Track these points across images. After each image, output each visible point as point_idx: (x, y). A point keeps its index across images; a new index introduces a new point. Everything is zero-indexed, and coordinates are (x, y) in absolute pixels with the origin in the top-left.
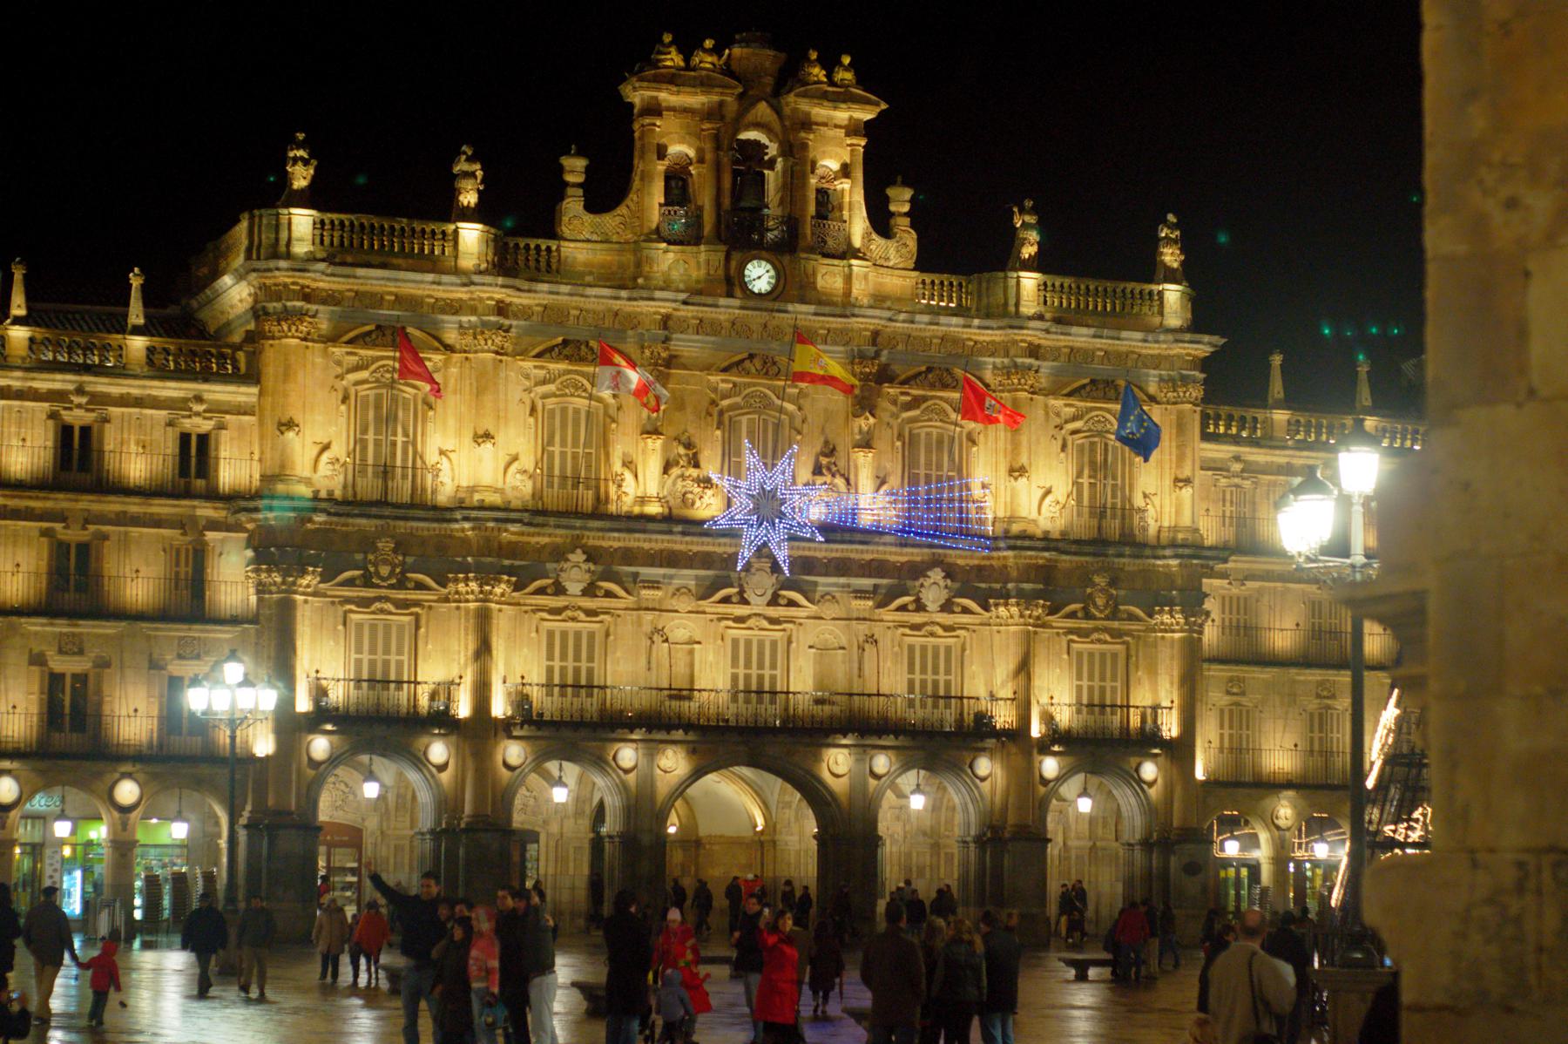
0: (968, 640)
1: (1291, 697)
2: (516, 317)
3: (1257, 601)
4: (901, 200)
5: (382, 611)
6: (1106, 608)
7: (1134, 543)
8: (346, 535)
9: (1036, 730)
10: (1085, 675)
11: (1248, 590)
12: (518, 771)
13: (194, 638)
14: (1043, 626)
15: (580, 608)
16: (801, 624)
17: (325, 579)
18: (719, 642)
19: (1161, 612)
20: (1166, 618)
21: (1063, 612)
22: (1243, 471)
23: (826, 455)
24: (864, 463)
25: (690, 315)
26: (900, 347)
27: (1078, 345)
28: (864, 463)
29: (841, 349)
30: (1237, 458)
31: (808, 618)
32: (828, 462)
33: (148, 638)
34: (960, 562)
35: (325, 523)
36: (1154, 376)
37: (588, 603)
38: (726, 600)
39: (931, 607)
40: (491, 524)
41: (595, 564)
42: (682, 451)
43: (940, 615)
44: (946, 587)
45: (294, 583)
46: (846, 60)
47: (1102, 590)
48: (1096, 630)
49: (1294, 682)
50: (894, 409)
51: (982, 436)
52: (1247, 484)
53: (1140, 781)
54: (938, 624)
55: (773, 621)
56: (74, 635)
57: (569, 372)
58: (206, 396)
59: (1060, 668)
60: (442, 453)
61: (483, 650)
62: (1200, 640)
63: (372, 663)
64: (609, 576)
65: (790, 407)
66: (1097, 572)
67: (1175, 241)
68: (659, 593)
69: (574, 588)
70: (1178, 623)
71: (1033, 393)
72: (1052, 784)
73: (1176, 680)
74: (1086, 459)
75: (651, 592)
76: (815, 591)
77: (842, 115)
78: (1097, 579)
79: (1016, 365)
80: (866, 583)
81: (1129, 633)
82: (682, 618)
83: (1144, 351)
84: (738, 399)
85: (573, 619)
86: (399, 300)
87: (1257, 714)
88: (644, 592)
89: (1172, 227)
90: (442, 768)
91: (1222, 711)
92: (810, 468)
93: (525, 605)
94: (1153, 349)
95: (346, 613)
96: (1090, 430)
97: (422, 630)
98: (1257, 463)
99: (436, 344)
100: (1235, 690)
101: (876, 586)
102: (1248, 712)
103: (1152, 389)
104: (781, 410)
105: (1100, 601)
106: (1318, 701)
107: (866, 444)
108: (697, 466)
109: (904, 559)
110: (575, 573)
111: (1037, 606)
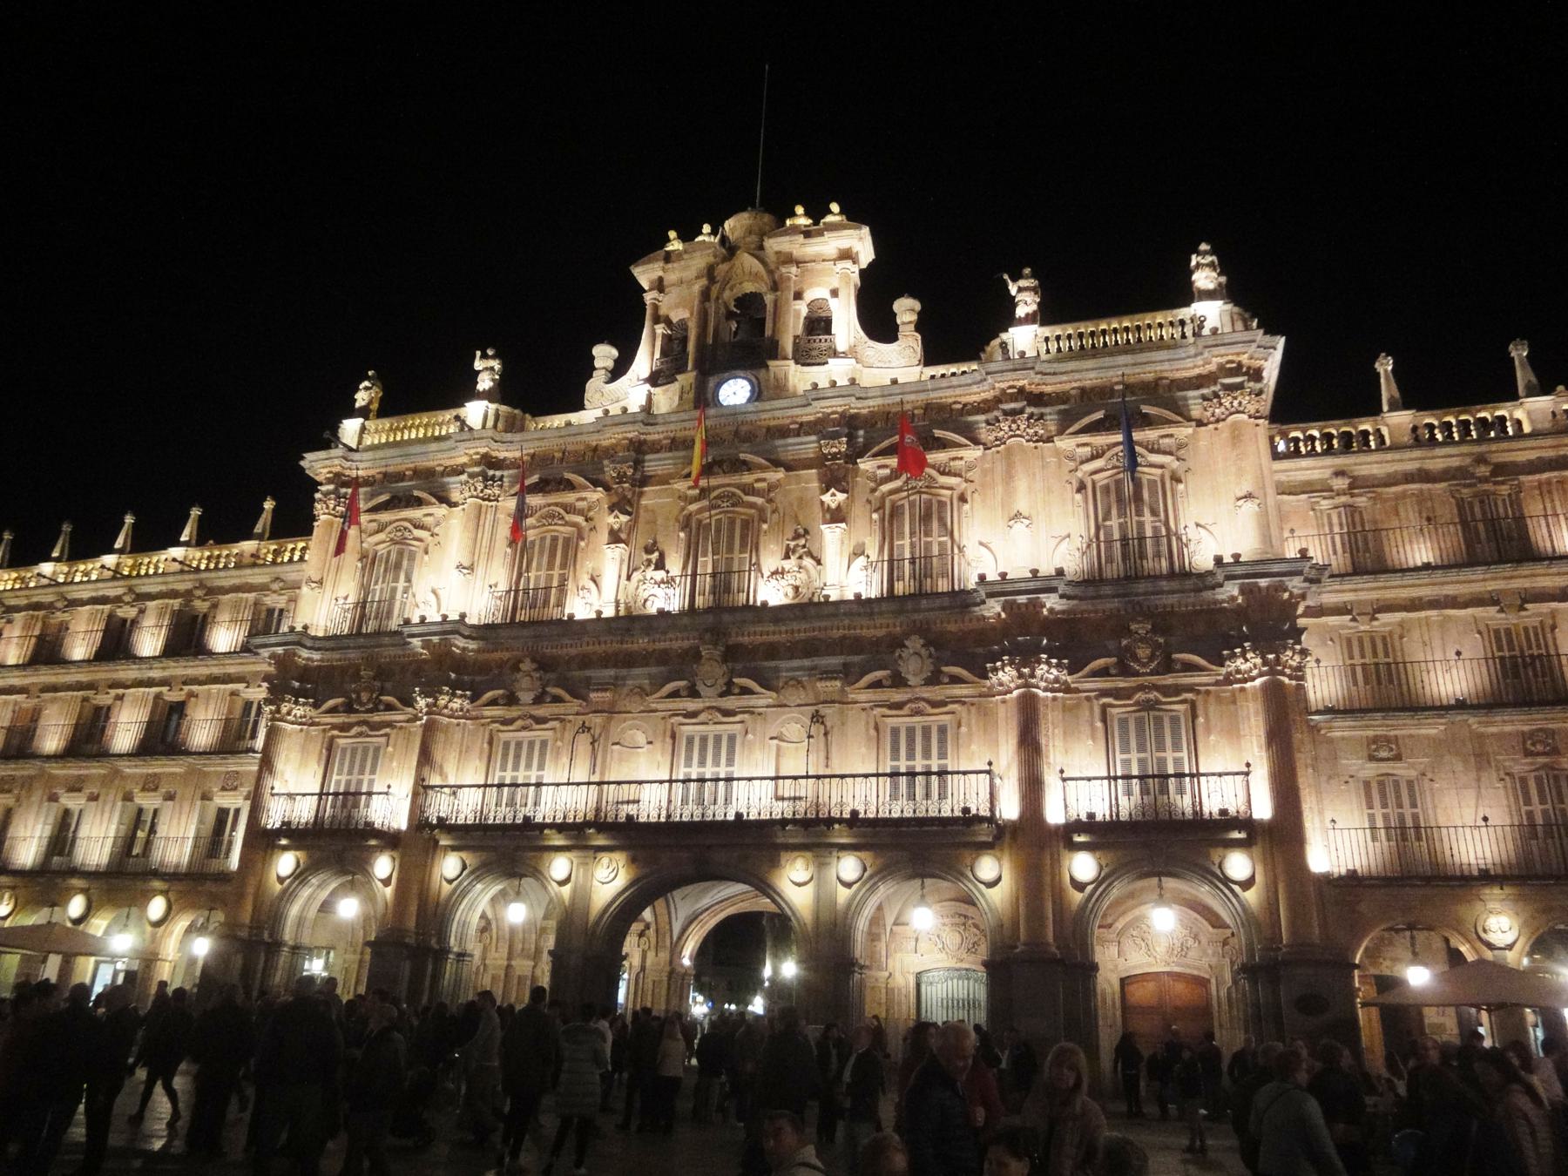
0: (964, 715)
1: (1480, 757)
2: (508, 468)
3: (1401, 637)
4: (906, 310)
5: (360, 735)
6: (1151, 658)
7: (1183, 576)
8: (343, 670)
9: (1054, 815)
10: (1133, 744)
11: (1385, 625)
12: (455, 883)
13: (237, 773)
14: (1067, 689)
15: (532, 717)
16: (760, 714)
17: (316, 706)
18: (669, 740)
19: (1233, 656)
20: (1240, 661)
21: (1087, 669)
22: (1352, 486)
23: (794, 539)
24: (832, 538)
25: (661, 436)
26: (879, 425)
27: (1088, 383)
28: (832, 538)
29: (814, 438)
30: (1339, 473)
31: (767, 707)
32: (802, 545)
33: (206, 774)
34: (952, 627)
35: (322, 660)
36: (1195, 398)
37: (541, 711)
38: (675, 694)
39: (912, 681)
40: (436, 639)
41: (546, 671)
42: (645, 557)
43: (924, 688)
44: (930, 656)
45: (278, 711)
46: (835, 207)
47: (1142, 640)
48: (1141, 688)
49: (1481, 736)
50: (872, 485)
51: (976, 495)
52: (1361, 501)
53: (1226, 881)
54: (924, 700)
55: (727, 713)
56: (155, 774)
57: (549, 505)
58: (282, 576)
59: (1093, 738)
60: (434, 592)
61: (426, 758)
62: (1300, 688)
63: (348, 783)
64: (562, 683)
65: (759, 501)
66: (1133, 620)
67: (1211, 265)
68: (607, 696)
69: (526, 697)
70: (1255, 666)
71: (1037, 441)
72: (1090, 888)
73: (1263, 740)
74: (1113, 497)
75: (600, 694)
76: (778, 678)
77: (829, 244)
78: (1133, 627)
79: (1006, 413)
80: (835, 661)
81: (1190, 688)
82: (634, 719)
83: (1178, 375)
84: (705, 503)
85: (524, 728)
86: (417, 473)
87: (1426, 784)
88: (593, 695)
89: (1205, 253)
90: (386, 882)
91: (1367, 784)
92: (780, 553)
93: (483, 718)
94: (1190, 365)
95: (332, 738)
96: (1113, 468)
97: (390, 749)
98: (1374, 477)
99: (434, 500)
100: (1383, 754)
101: (845, 665)
102: (1410, 784)
103: (1196, 412)
104: (752, 505)
105: (1143, 652)
106: (1529, 760)
107: (837, 516)
108: (660, 565)
109: (881, 633)
110: (525, 682)
111: (1039, 662)
